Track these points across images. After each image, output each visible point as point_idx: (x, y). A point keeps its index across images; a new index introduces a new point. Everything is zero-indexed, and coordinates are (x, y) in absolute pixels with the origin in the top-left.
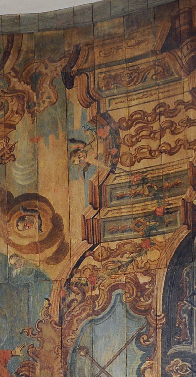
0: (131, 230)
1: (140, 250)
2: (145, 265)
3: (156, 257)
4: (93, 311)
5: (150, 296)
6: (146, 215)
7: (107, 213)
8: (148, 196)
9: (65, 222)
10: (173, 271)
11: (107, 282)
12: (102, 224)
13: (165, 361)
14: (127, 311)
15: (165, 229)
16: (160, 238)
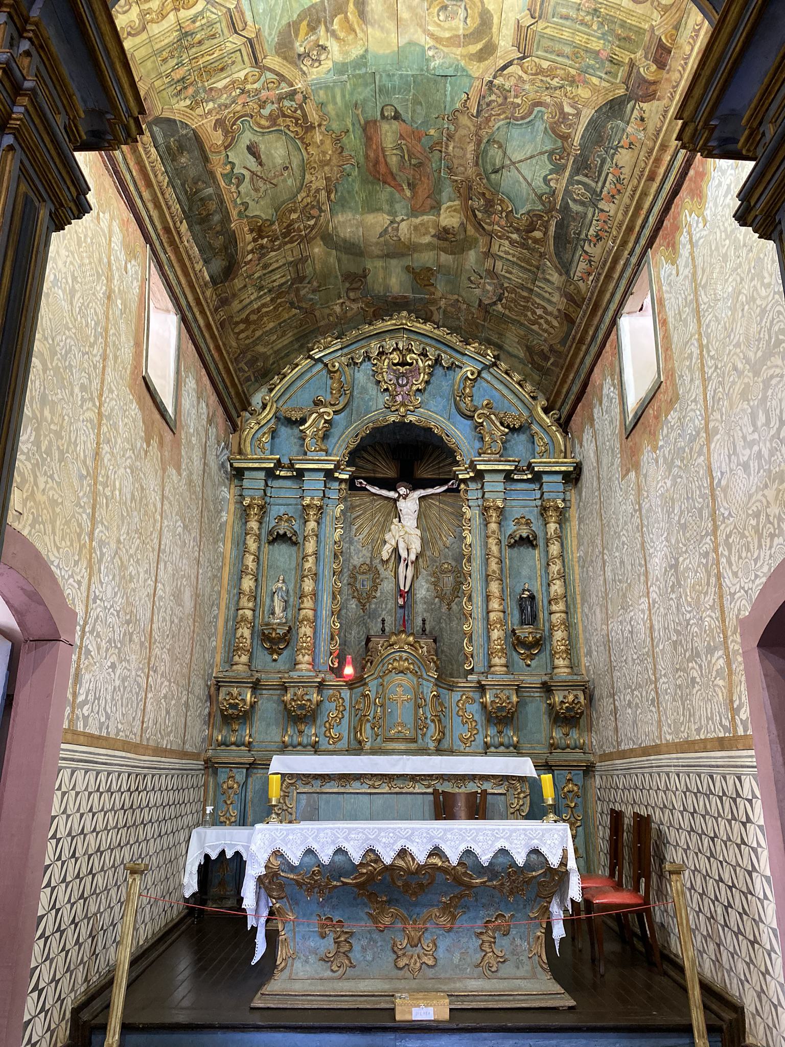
0: (568, 57)
1: (573, 82)
2: (573, 98)
3: (587, 96)
4: (512, 115)
5: (570, 126)
6: (587, 50)
7: (546, 28)
8: (595, 31)
9: (496, 20)
10: (599, 117)
11: (532, 95)
12: (537, 38)
13: (570, 182)
14: (546, 128)
15: (604, 76)
16: (595, 80)
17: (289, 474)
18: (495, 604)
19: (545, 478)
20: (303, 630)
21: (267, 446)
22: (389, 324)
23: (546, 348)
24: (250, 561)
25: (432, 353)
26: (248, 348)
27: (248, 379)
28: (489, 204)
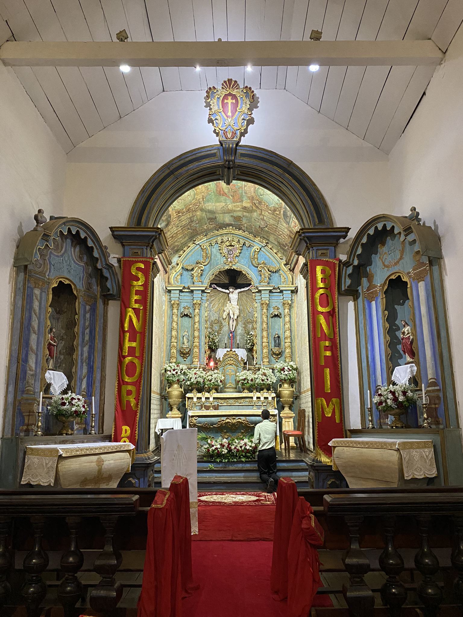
17: (188, 291)
18: (265, 340)
19: (284, 292)
20: (195, 350)
21: (179, 281)
22: (225, 231)
23: (284, 244)
24: (174, 324)
25: (242, 242)
26: (172, 244)
27: (171, 254)
28: (260, 203)
